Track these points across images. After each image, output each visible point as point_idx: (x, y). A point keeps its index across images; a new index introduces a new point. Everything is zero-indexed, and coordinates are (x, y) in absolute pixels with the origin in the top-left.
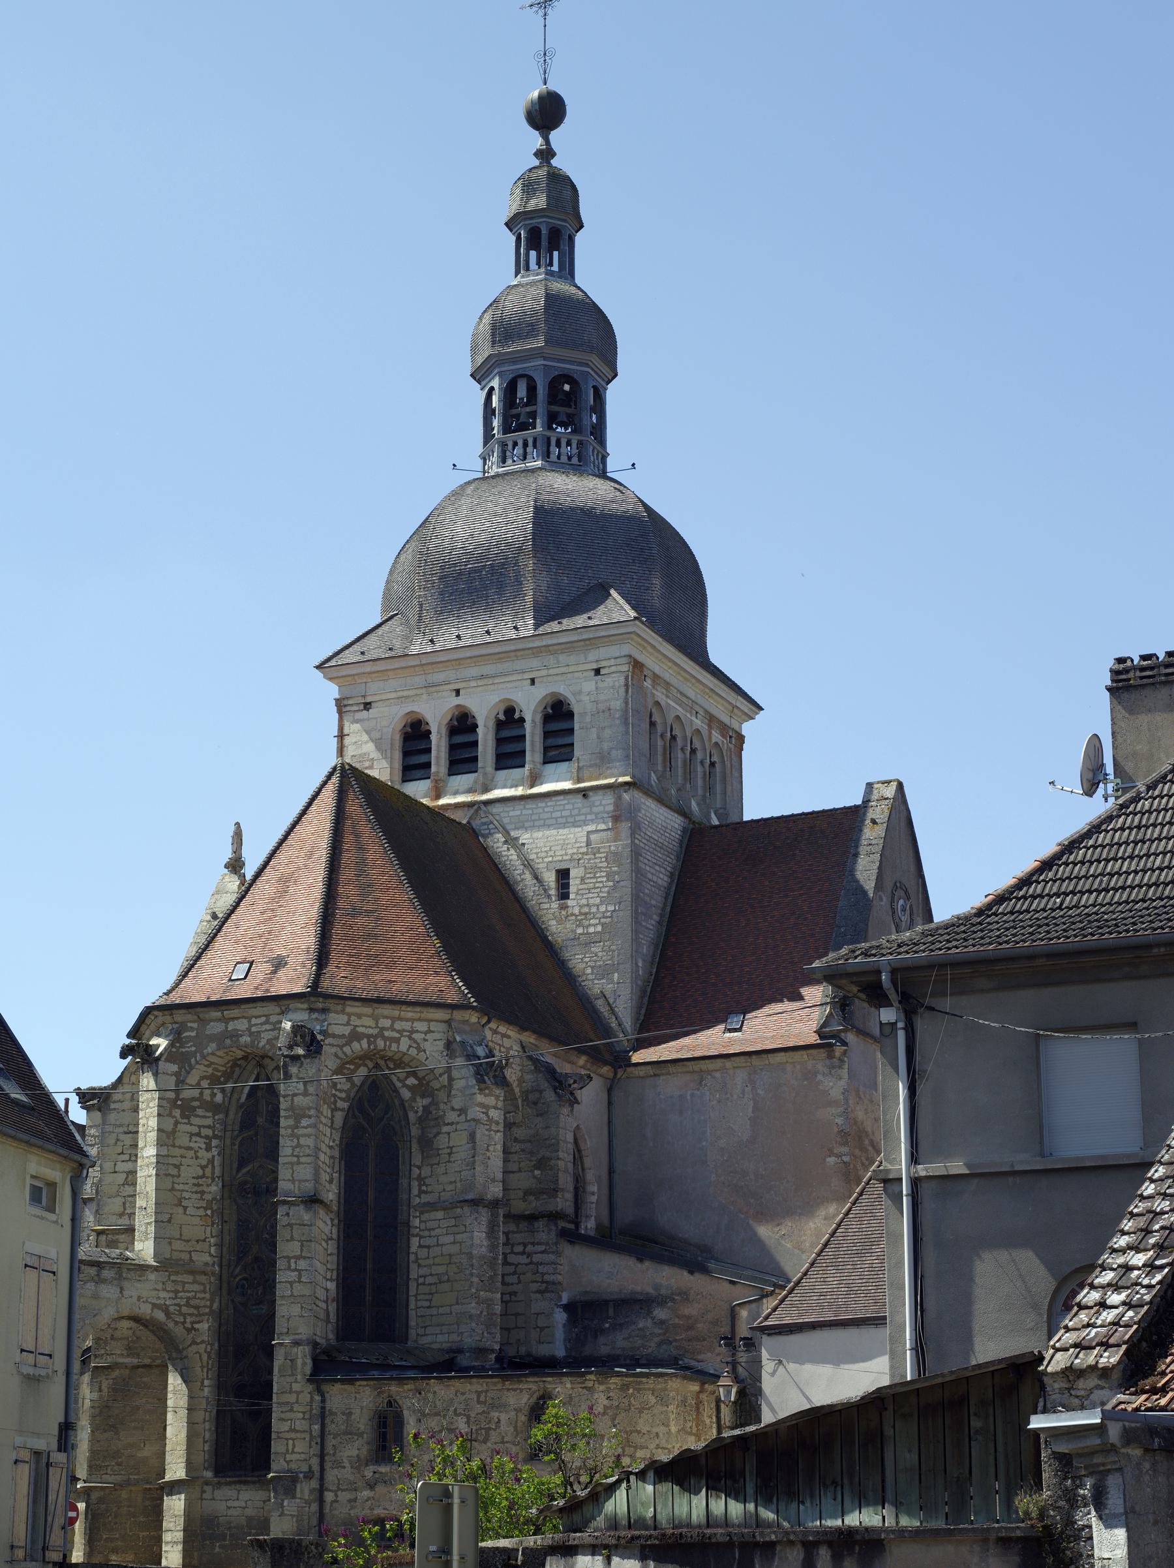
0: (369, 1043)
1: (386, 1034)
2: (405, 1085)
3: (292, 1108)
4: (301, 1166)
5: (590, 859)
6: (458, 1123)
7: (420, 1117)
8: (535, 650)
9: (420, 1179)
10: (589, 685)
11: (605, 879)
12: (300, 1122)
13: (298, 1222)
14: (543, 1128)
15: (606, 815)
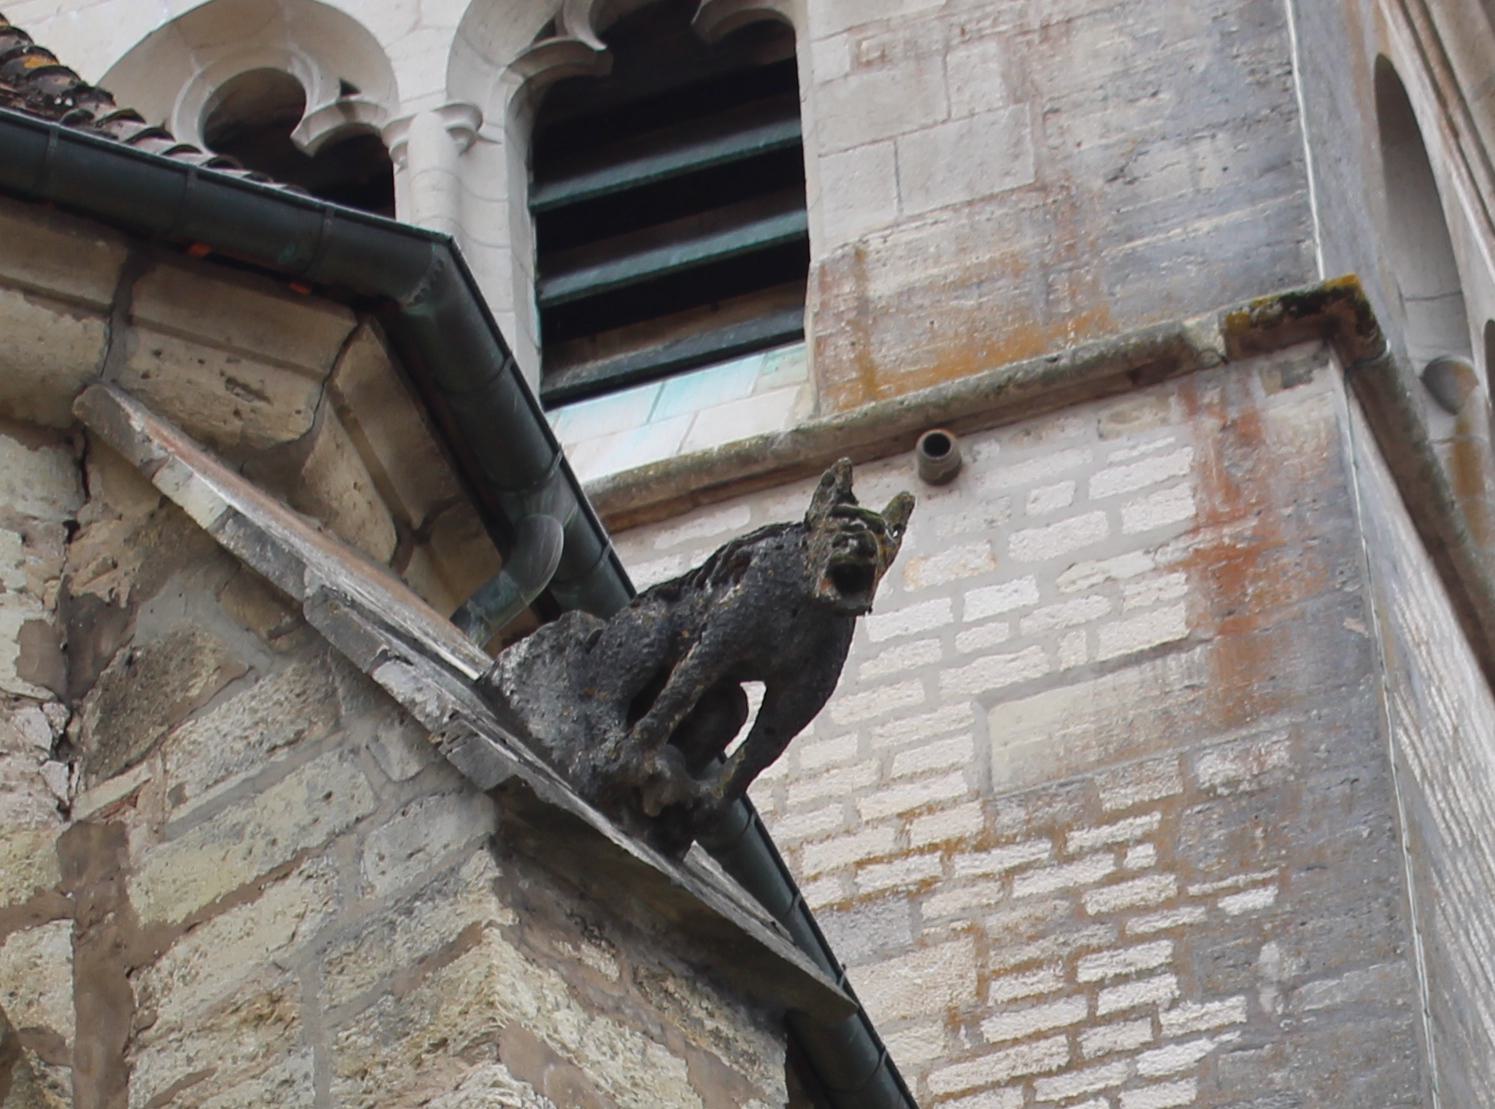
5: (1010, 875)
11: (1165, 986)
15: (1140, 562)
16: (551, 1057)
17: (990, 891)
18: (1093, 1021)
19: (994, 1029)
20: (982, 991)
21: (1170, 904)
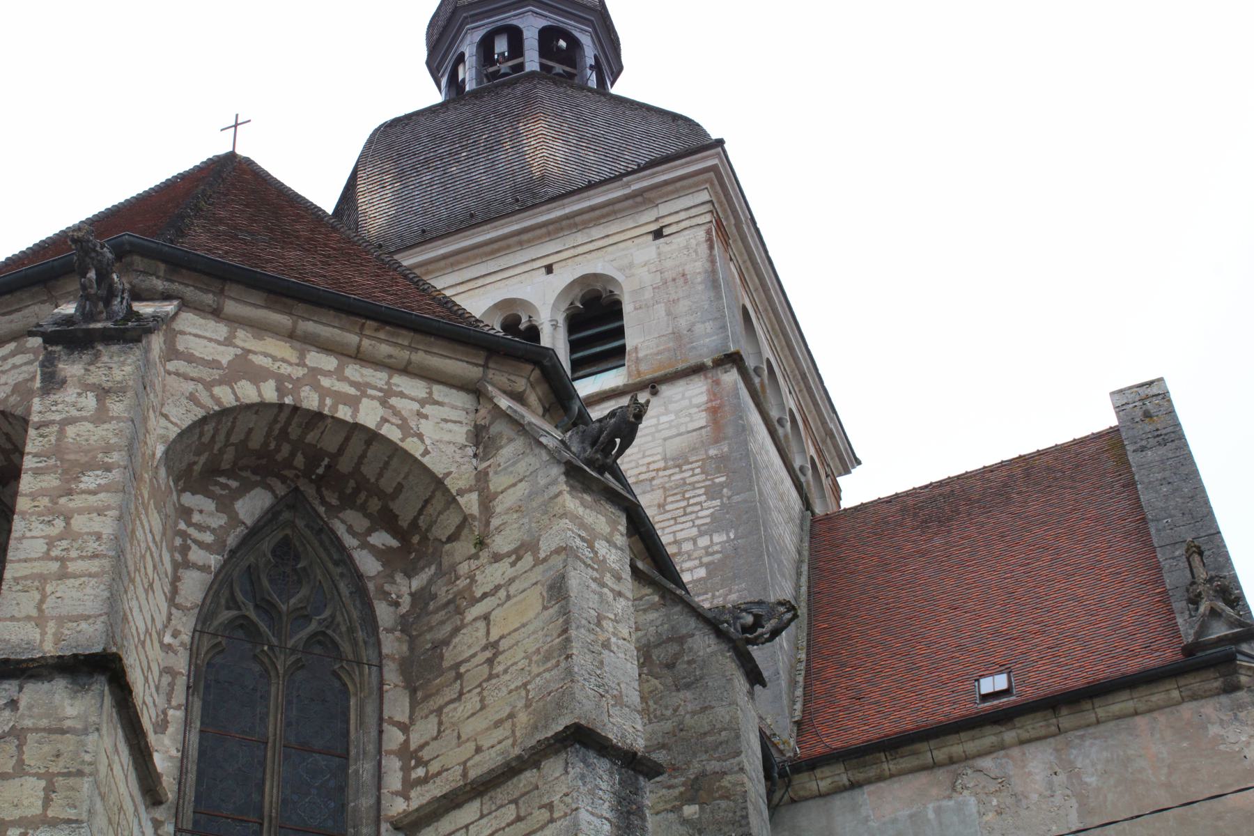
0: (280, 390)
1: (326, 382)
2: (365, 545)
3: (57, 450)
4: (70, 582)
5: (670, 476)
6: (512, 581)
7: (403, 616)
8: (551, 228)
9: (409, 756)
10: (647, 251)
12: (77, 479)
13: (44, 723)
14: (694, 713)
15: (696, 410)
16: (577, 518)
17: (666, 479)
18: (689, 505)
19: (668, 507)
20: (665, 500)
21: (704, 481)
